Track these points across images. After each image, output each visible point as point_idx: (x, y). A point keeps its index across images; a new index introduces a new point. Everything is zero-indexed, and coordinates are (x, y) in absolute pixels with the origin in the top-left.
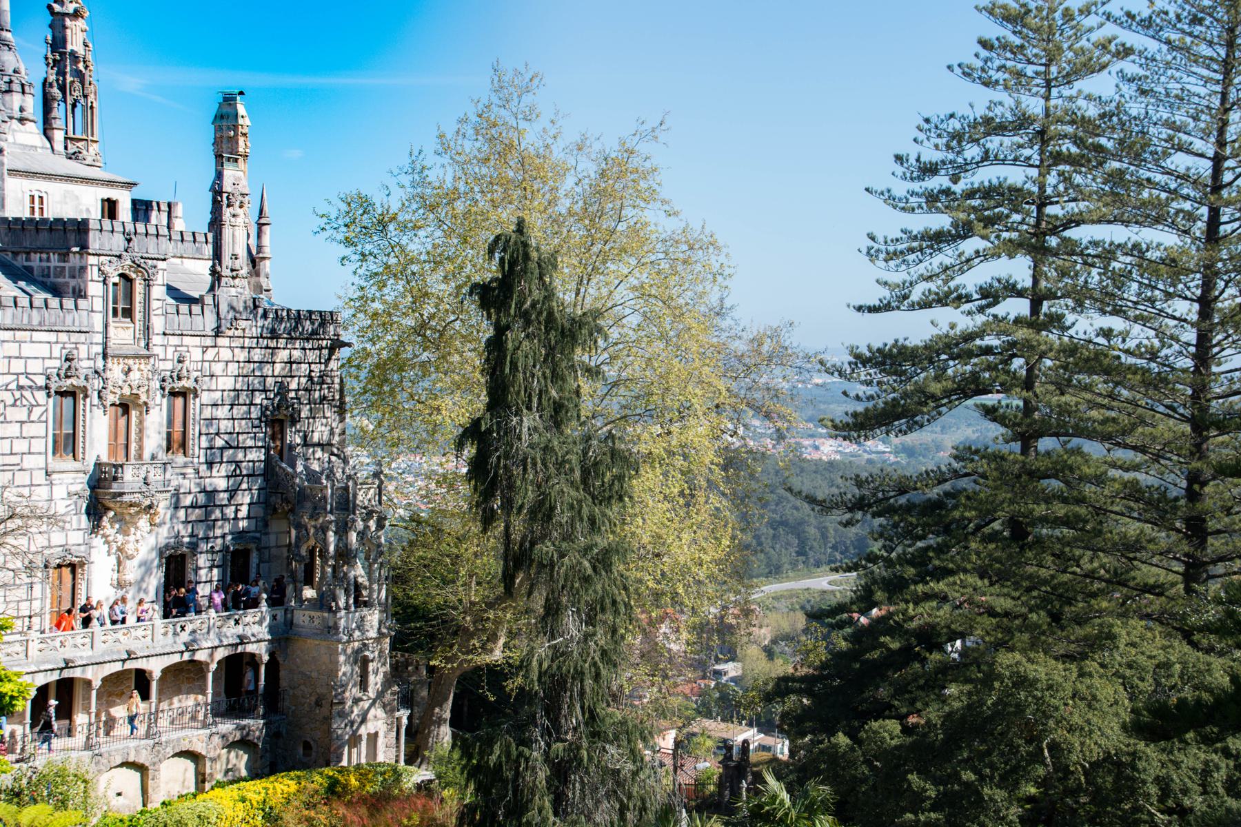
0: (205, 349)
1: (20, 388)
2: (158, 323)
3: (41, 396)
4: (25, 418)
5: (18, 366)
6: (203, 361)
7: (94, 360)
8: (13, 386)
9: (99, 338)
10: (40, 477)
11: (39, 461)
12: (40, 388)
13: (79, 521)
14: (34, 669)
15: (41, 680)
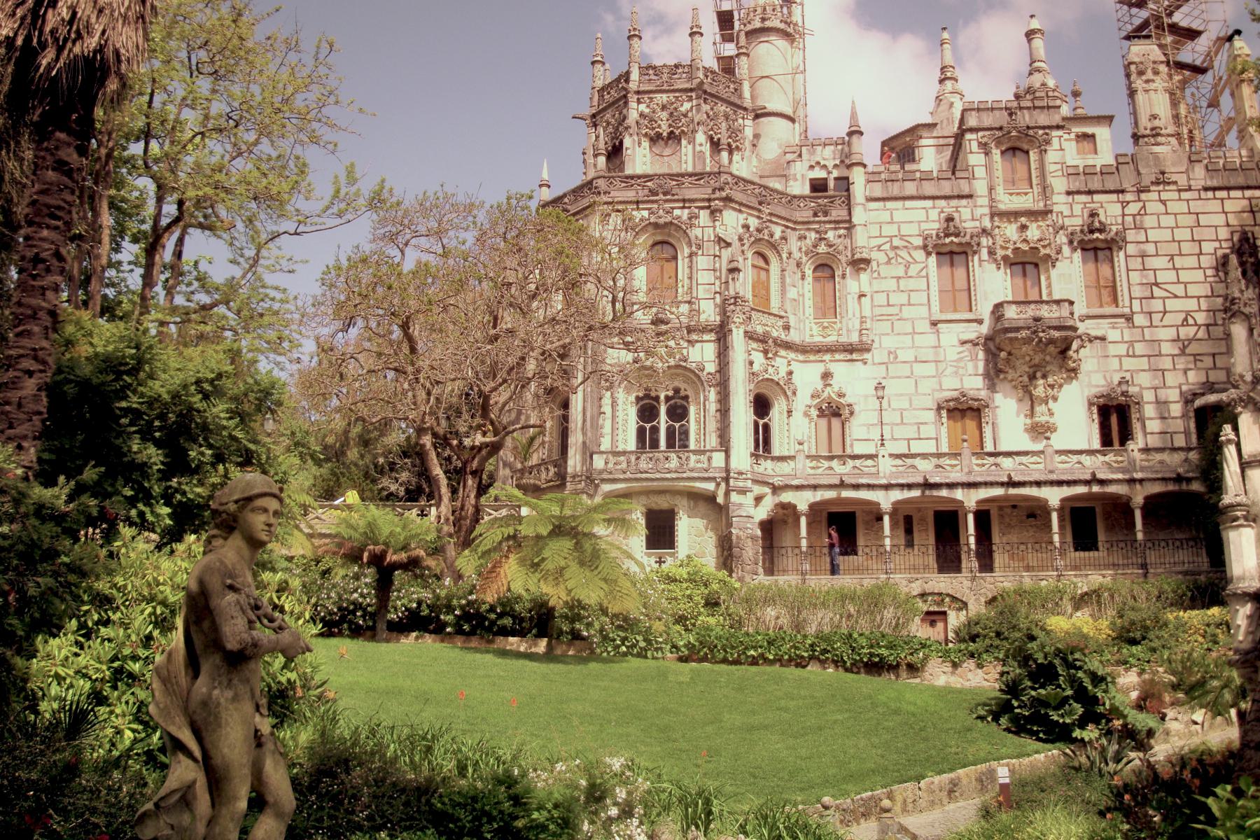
0: (1125, 204)
1: (895, 248)
2: (1059, 184)
3: (920, 255)
4: (902, 274)
5: (890, 230)
6: (1124, 215)
7: (980, 220)
8: (887, 247)
9: (985, 201)
10: (924, 326)
11: (923, 311)
12: (916, 248)
13: (976, 367)
14: (884, 481)
15: (897, 495)
